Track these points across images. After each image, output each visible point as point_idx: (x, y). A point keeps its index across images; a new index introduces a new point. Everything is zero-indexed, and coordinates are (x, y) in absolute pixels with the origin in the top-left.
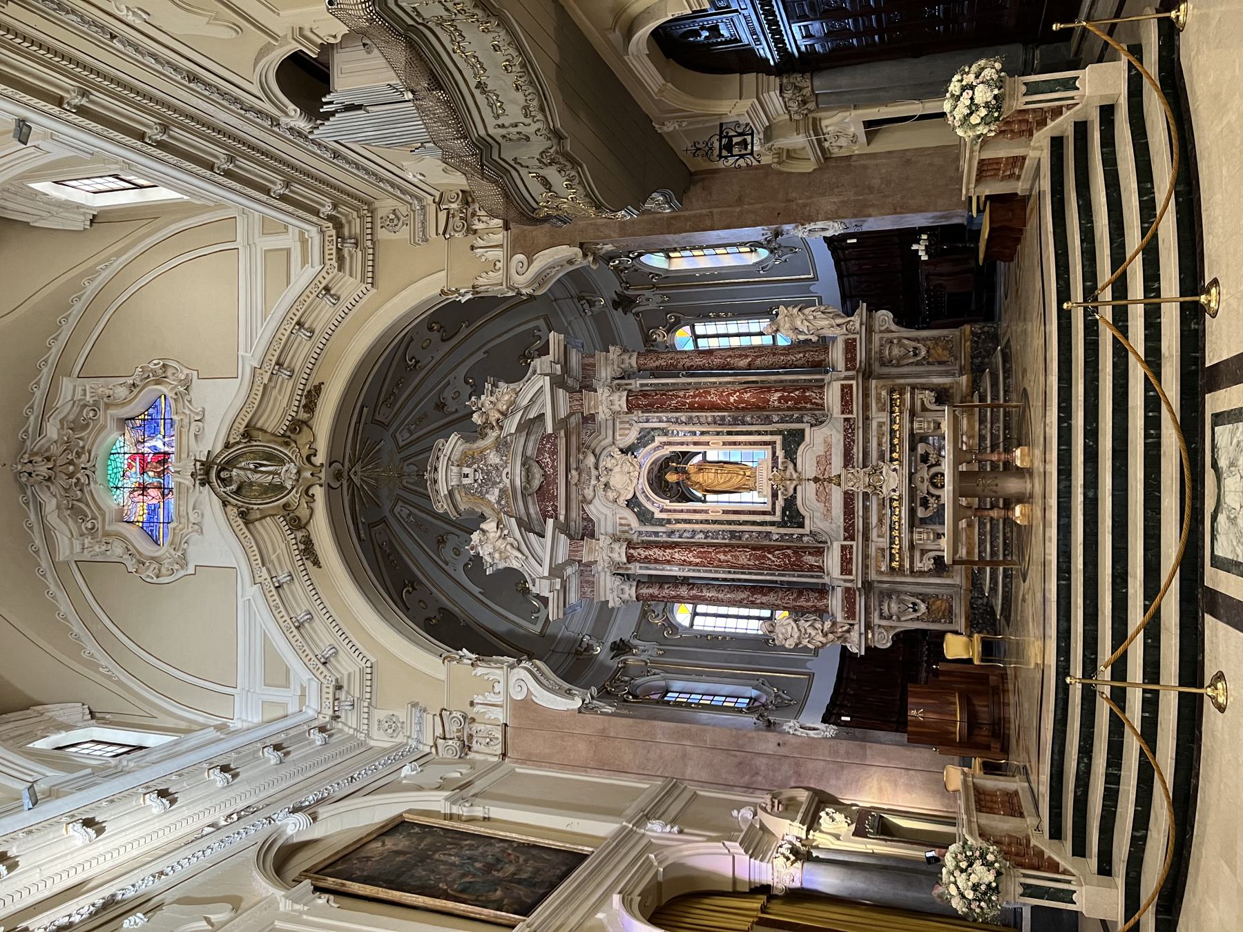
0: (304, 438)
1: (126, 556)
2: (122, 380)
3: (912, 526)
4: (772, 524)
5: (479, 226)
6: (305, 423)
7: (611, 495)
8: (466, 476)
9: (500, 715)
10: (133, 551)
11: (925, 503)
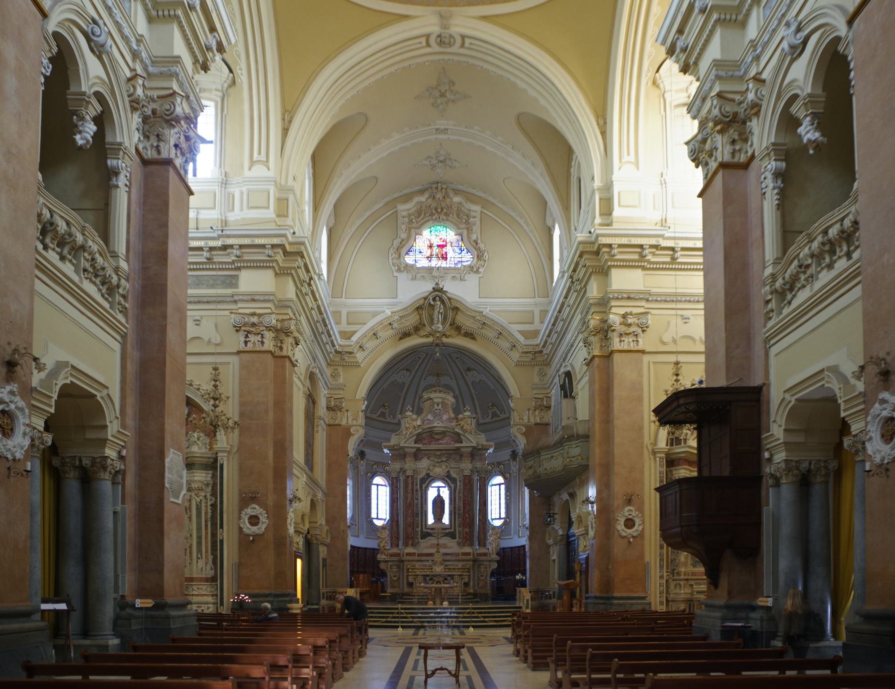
0: (453, 332)
3: (424, 575)
4: (422, 528)
5: (537, 412)
6: (460, 333)
7: (431, 468)
8: (438, 405)
9: (344, 422)
10: (403, 243)
11: (431, 579)
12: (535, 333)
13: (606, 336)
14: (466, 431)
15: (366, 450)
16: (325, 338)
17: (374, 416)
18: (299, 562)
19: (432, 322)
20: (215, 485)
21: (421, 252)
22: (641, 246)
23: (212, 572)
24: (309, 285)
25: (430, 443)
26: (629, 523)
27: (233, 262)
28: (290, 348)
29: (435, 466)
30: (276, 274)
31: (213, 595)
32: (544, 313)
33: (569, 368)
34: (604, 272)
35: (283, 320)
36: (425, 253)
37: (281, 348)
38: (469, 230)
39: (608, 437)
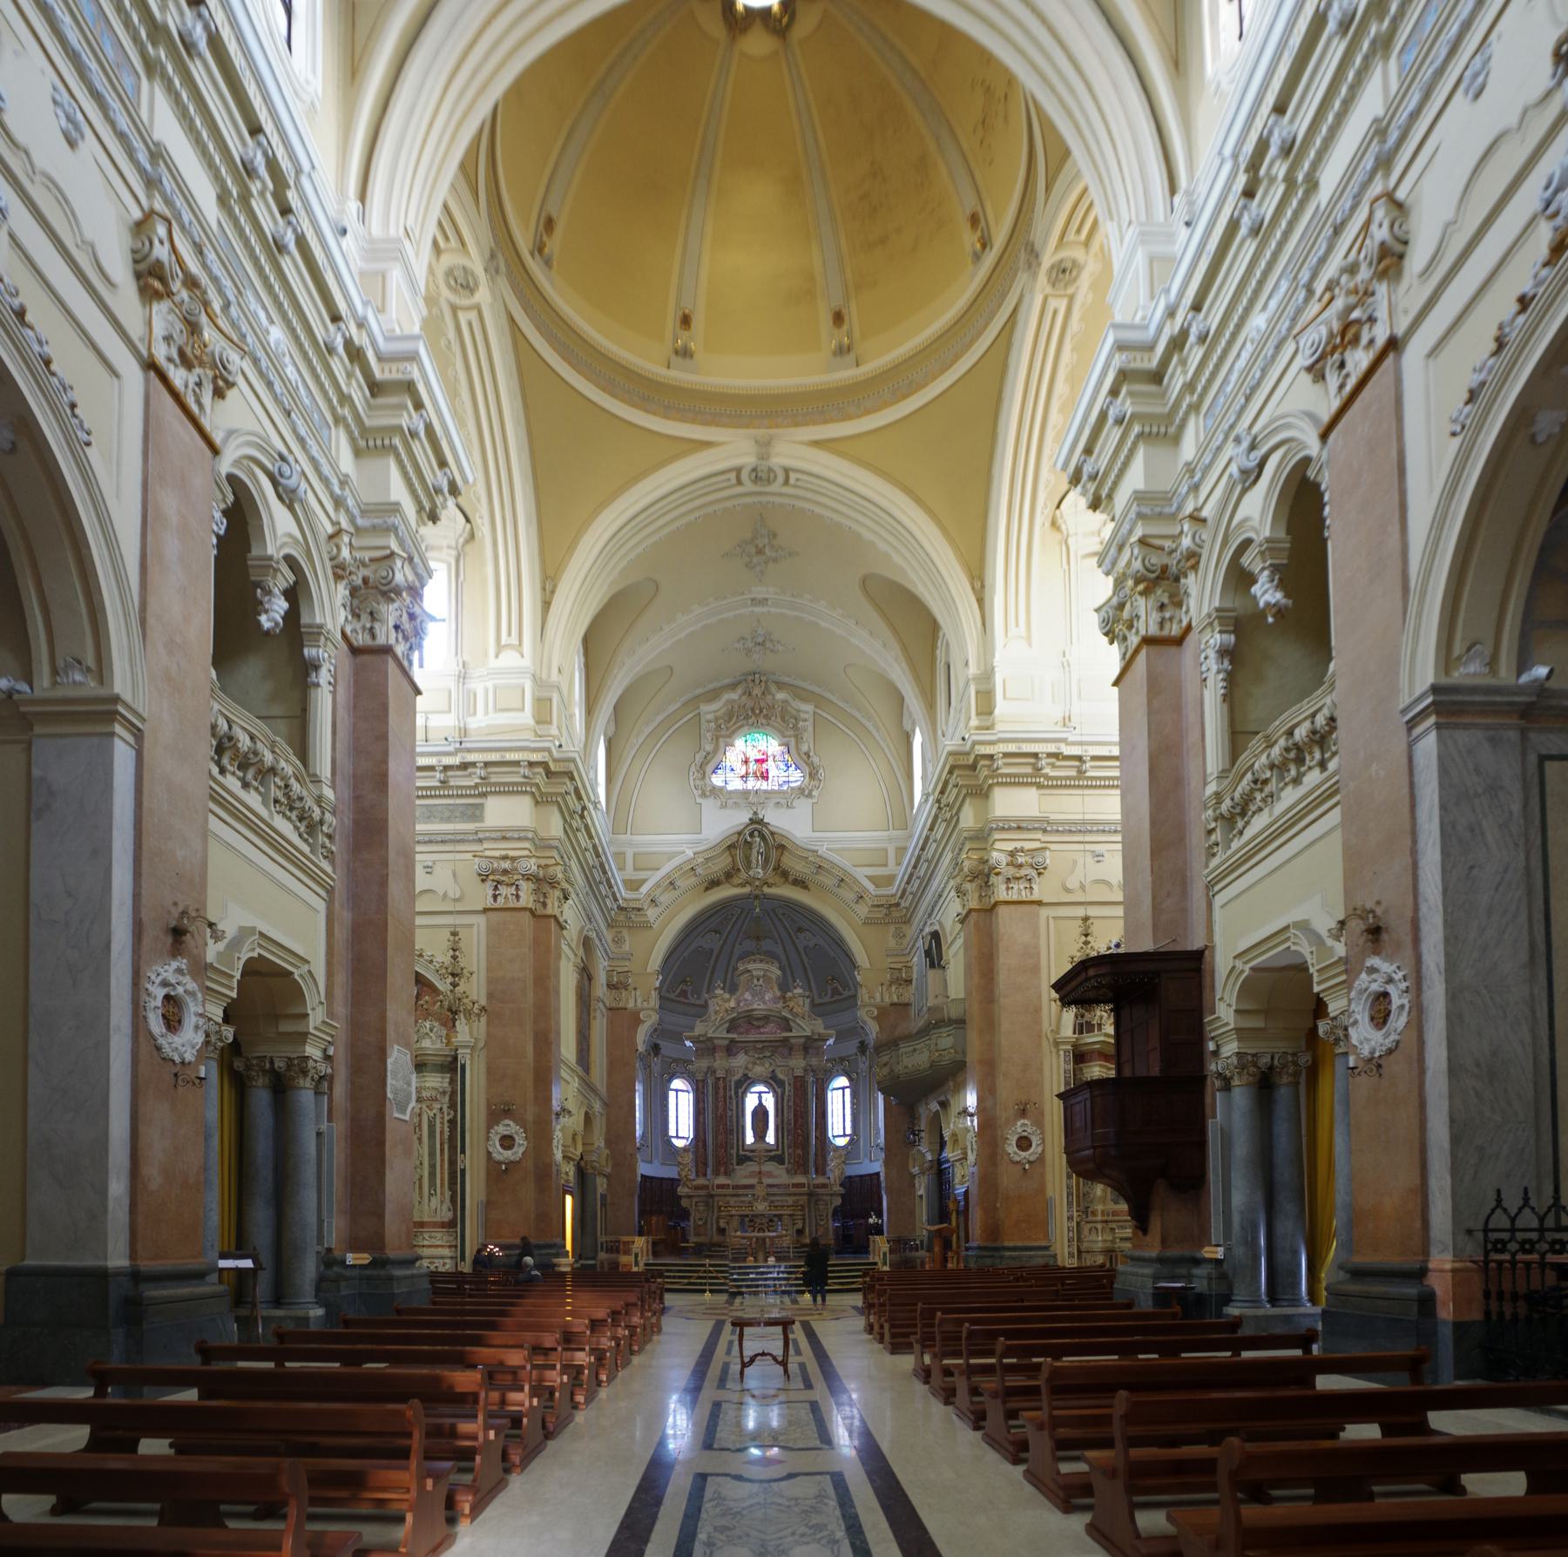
0: (778, 879)
5: (893, 988)
6: (787, 880)
7: (750, 1066)
9: (631, 1005)
12: (890, 879)
13: (987, 883)
14: (796, 1015)
15: (662, 1043)
16: (603, 889)
17: (672, 996)
18: (569, 1199)
19: (748, 866)
20: (453, 1093)
22: (1035, 755)
23: (450, 1215)
24: (582, 817)
25: (747, 1032)
26: (1024, 1143)
27: (476, 786)
28: (556, 904)
29: (755, 1064)
30: (537, 803)
31: (450, 1247)
32: (901, 851)
33: (937, 927)
34: (982, 793)
35: (547, 866)
37: (544, 905)
38: (798, 738)
39: (990, 1024)
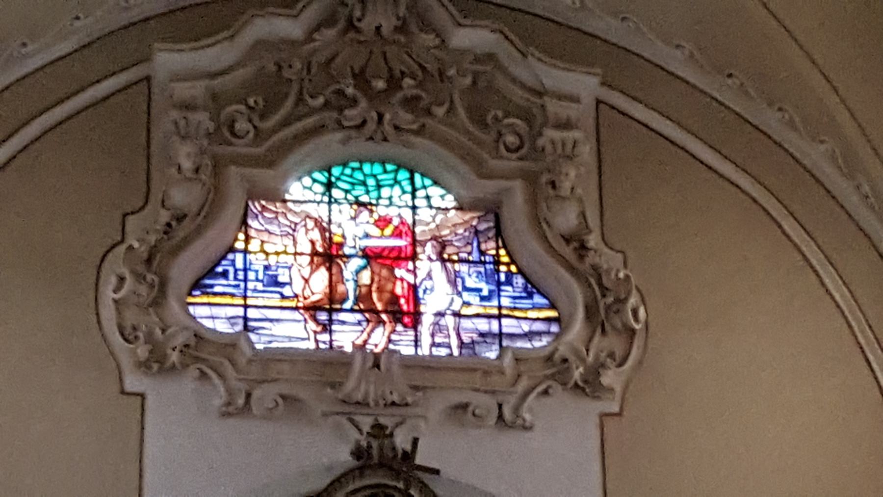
1: (164, 216)
2: (593, 220)
10: (181, 232)
21: (275, 282)
36: (298, 286)
